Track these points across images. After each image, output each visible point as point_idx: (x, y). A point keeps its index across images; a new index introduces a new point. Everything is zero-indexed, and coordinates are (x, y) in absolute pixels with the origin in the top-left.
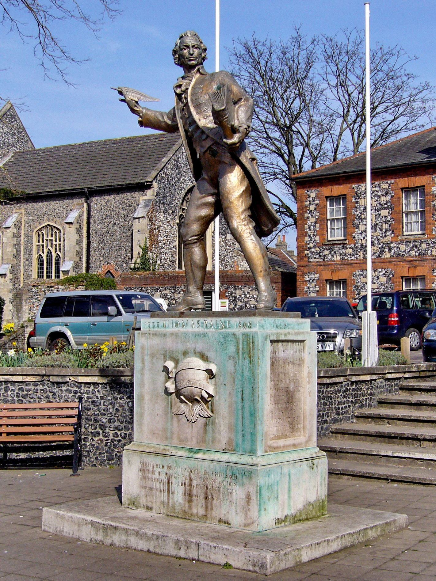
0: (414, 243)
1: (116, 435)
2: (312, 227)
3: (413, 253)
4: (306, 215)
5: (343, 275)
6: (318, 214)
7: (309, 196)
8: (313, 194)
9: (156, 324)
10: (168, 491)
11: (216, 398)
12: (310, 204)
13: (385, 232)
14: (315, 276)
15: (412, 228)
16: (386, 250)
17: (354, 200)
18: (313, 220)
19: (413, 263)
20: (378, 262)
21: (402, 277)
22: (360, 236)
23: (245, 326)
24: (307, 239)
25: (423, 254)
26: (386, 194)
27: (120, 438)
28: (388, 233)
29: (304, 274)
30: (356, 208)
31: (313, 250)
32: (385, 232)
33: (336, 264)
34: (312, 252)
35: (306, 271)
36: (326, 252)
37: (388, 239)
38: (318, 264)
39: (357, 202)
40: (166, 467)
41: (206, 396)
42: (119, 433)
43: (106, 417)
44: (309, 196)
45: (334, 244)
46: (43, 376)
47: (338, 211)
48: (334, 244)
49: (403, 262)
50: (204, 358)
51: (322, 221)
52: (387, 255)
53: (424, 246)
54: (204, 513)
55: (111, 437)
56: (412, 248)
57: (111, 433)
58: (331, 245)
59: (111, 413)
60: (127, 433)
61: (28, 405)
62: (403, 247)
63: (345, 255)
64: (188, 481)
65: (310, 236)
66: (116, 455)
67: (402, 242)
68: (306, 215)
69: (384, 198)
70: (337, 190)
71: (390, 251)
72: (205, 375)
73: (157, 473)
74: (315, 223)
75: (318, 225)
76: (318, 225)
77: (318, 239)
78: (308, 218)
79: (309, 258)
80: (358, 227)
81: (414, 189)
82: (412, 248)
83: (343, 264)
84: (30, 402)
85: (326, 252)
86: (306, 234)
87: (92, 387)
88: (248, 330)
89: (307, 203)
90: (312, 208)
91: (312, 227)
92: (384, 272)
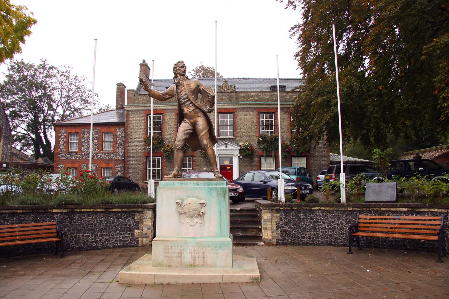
0: (108, 153)
1: (71, 237)
2: (62, 145)
3: (107, 158)
4: (60, 140)
5: (76, 165)
6: (65, 140)
7: (61, 132)
8: (63, 131)
9: (163, 184)
10: (181, 257)
11: (206, 215)
12: (62, 135)
13: (95, 149)
14: (63, 166)
15: (108, 148)
16: (96, 156)
17: (82, 135)
18: (62, 142)
19: (107, 162)
20: (93, 161)
21: (102, 167)
22: (84, 150)
23: (219, 184)
24: (59, 150)
25: (111, 158)
26: (96, 134)
27: (73, 238)
28: (97, 150)
29: (57, 165)
30: (83, 138)
31: (62, 154)
32: (95, 149)
33: (73, 161)
34: (61, 155)
35: (58, 163)
36: (68, 156)
37: (96, 152)
38: (64, 161)
39: (83, 136)
40: (179, 246)
41: (201, 214)
42: (73, 235)
43: (66, 228)
44: (61, 132)
45: (72, 153)
46: (34, 209)
47: (74, 138)
48: (72, 153)
49: (103, 161)
50: (198, 198)
51: (68, 143)
52: (96, 158)
53: (112, 155)
54: (202, 263)
55: (69, 238)
56: (107, 156)
57: (69, 236)
58: (71, 153)
59: (69, 226)
60: (78, 235)
61: (25, 225)
62: (103, 155)
63: (77, 157)
64: (193, 251)
65: (61, 149)
66: (72, 246)
67: (102, 153)
68: (60, 140)
69: (95, 135)
70: (74, 131)
71: (97, 156)
72: (200, 205)
73: (174, 250)
74: (64, 143)
75: (65, 144)
76: (65, 144)
77: (64, 150)
78: (60, 141)
79: (60, 158)
80: (83, 146)
81: (108, 133)
82: (107, 156)
83: (76, 161)
84: (26, 223)
85: (68, 156)
86: (59, 148)
87: (59, 215)
88: (221, 186)
89: (60, 135)
90: (63, 137)
91: (62, 145)
92: (94, 165)
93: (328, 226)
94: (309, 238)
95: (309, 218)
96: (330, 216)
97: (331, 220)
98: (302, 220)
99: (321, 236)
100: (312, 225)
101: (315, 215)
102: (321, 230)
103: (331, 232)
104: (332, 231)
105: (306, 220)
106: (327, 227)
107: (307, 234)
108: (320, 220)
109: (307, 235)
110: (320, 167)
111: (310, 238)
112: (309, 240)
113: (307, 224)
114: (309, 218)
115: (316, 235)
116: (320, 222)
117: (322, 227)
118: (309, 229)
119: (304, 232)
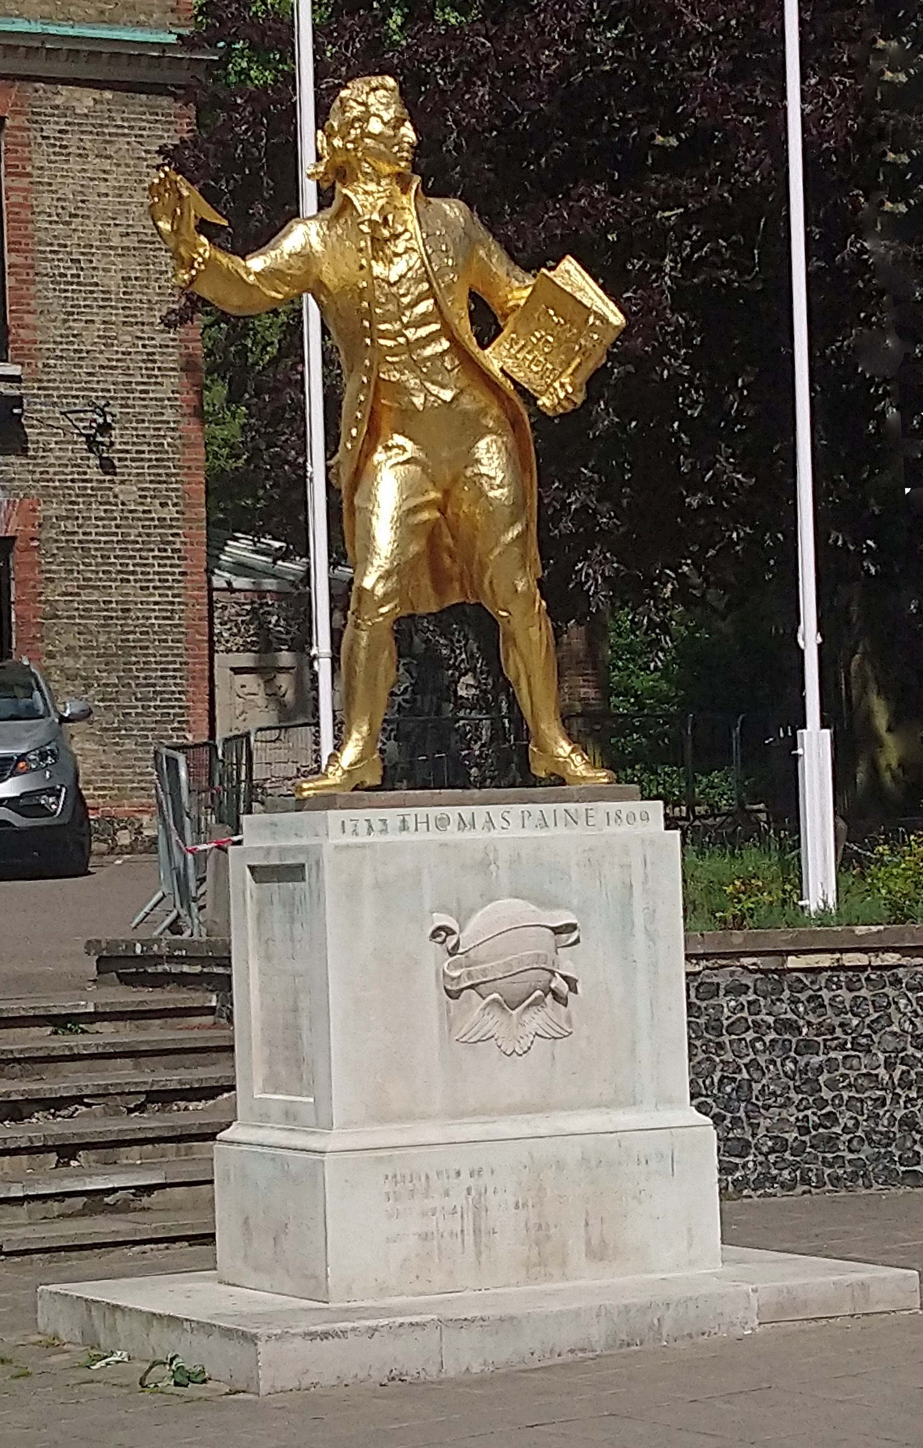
93: (889, 1065)
94: (772, 1150)
95: (771, 1020)
96: (903, 1002)
97: (907, 1026)
98: (726, 1039)
99: (845, 1129)
100: (790, 1066)
101: (810, 999)
102: (846, 1095)
103: (909, 1100)
104: (914, 1095)
105: (750, 1035)
106: (882, 1071)
107: (765, 1123)
108: (839, 1032)
109: (761, 1132)
110: (125, 649)
111: (781, 1145)
112: (772, 1158)
113: (762, 1060)
114: (771, 1020)
115: (816, 1127)
116: (842, 1047)
117: (853, 1074)
118: (774, 1093)
119: (741, 1114)
